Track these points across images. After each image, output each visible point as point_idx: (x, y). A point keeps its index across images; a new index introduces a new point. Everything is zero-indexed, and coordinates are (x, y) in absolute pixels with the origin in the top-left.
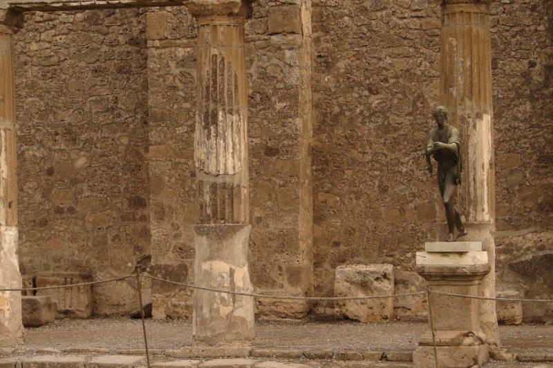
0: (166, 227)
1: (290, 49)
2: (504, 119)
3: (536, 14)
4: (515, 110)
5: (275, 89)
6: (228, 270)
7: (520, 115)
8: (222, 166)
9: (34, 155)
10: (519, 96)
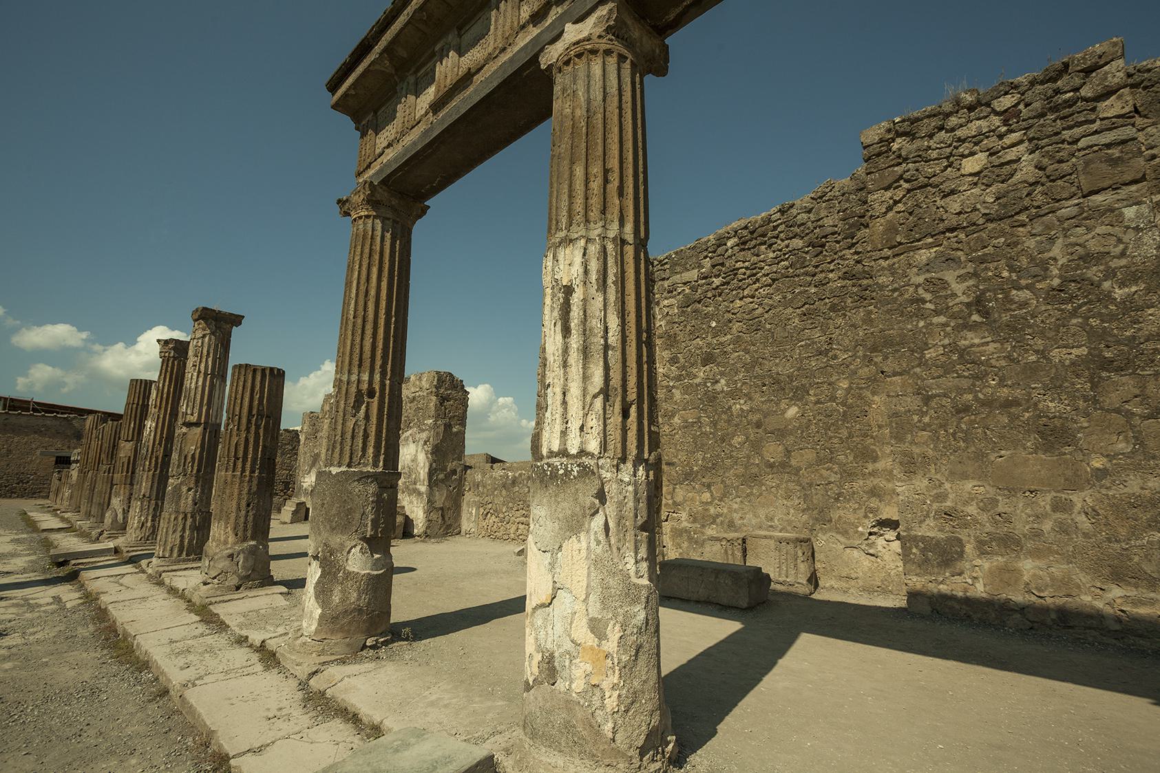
9: (741, 409)
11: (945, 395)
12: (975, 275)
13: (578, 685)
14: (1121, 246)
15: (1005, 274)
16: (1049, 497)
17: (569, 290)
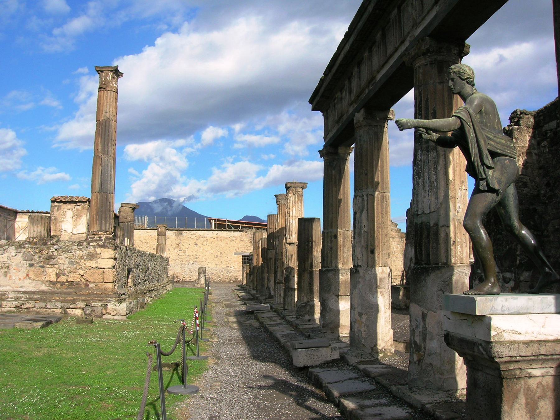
8: (420, 206)
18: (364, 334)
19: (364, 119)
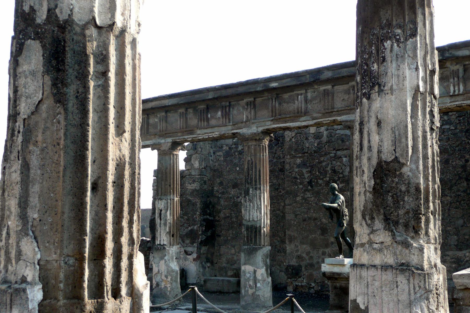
0: (293, 246)
1: (345, 157)
2: (453, 191)
3: (468, 134)
4: (459, 186)
5: (339, 178)
6: (253, 270)
7: (461, 189)
8: (251, 217)
10: (460, 178)
11: (301, 215)
12: (310, 172)
13: (163, 287)
14: (342, 170)
15: (317, 173)
16: (321, 250)
17: (161, 210)
18: (169, 289)
19: (169, 149)
